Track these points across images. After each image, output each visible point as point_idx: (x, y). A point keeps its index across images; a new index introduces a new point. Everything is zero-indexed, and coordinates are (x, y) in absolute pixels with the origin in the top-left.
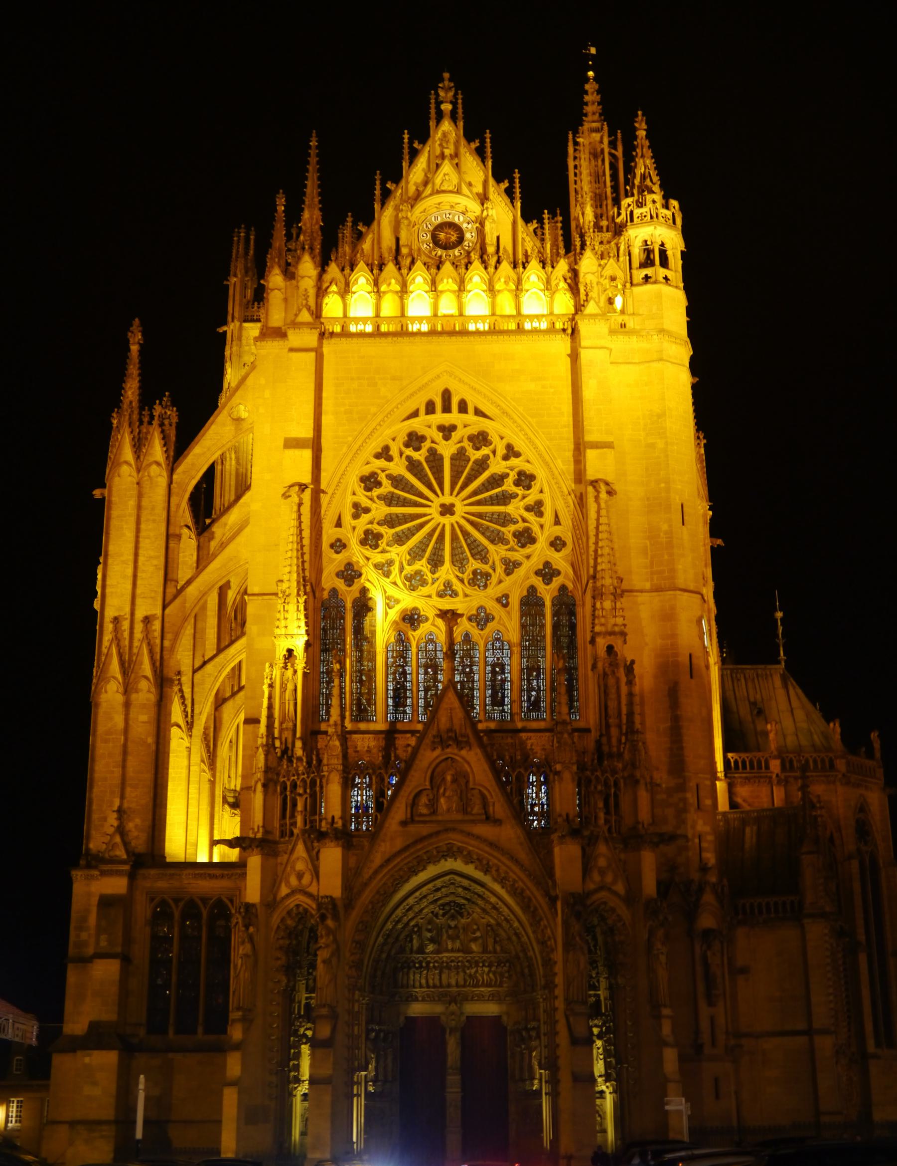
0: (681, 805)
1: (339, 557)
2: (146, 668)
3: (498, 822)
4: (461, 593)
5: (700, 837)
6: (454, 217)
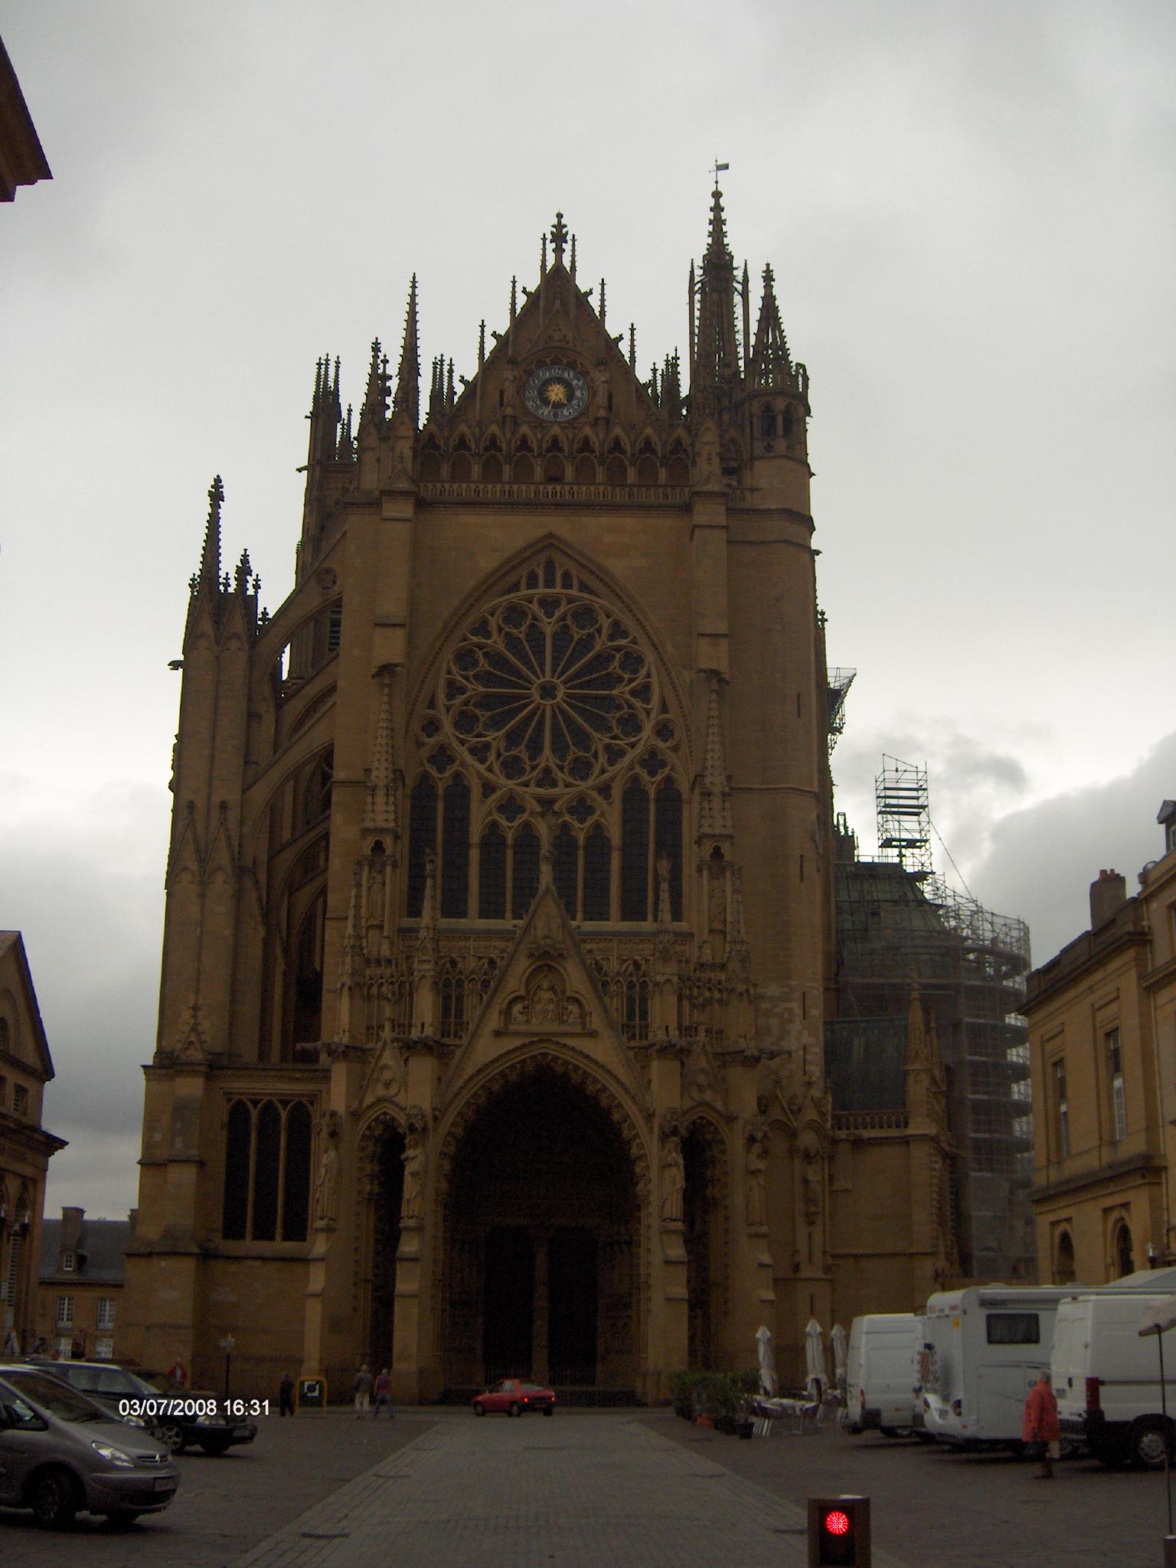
0: (786, 1015)
1: (432, 741)
3: (593, 1034)
4: (561, 784)
5: (804, 1048)
6: (563, 372)
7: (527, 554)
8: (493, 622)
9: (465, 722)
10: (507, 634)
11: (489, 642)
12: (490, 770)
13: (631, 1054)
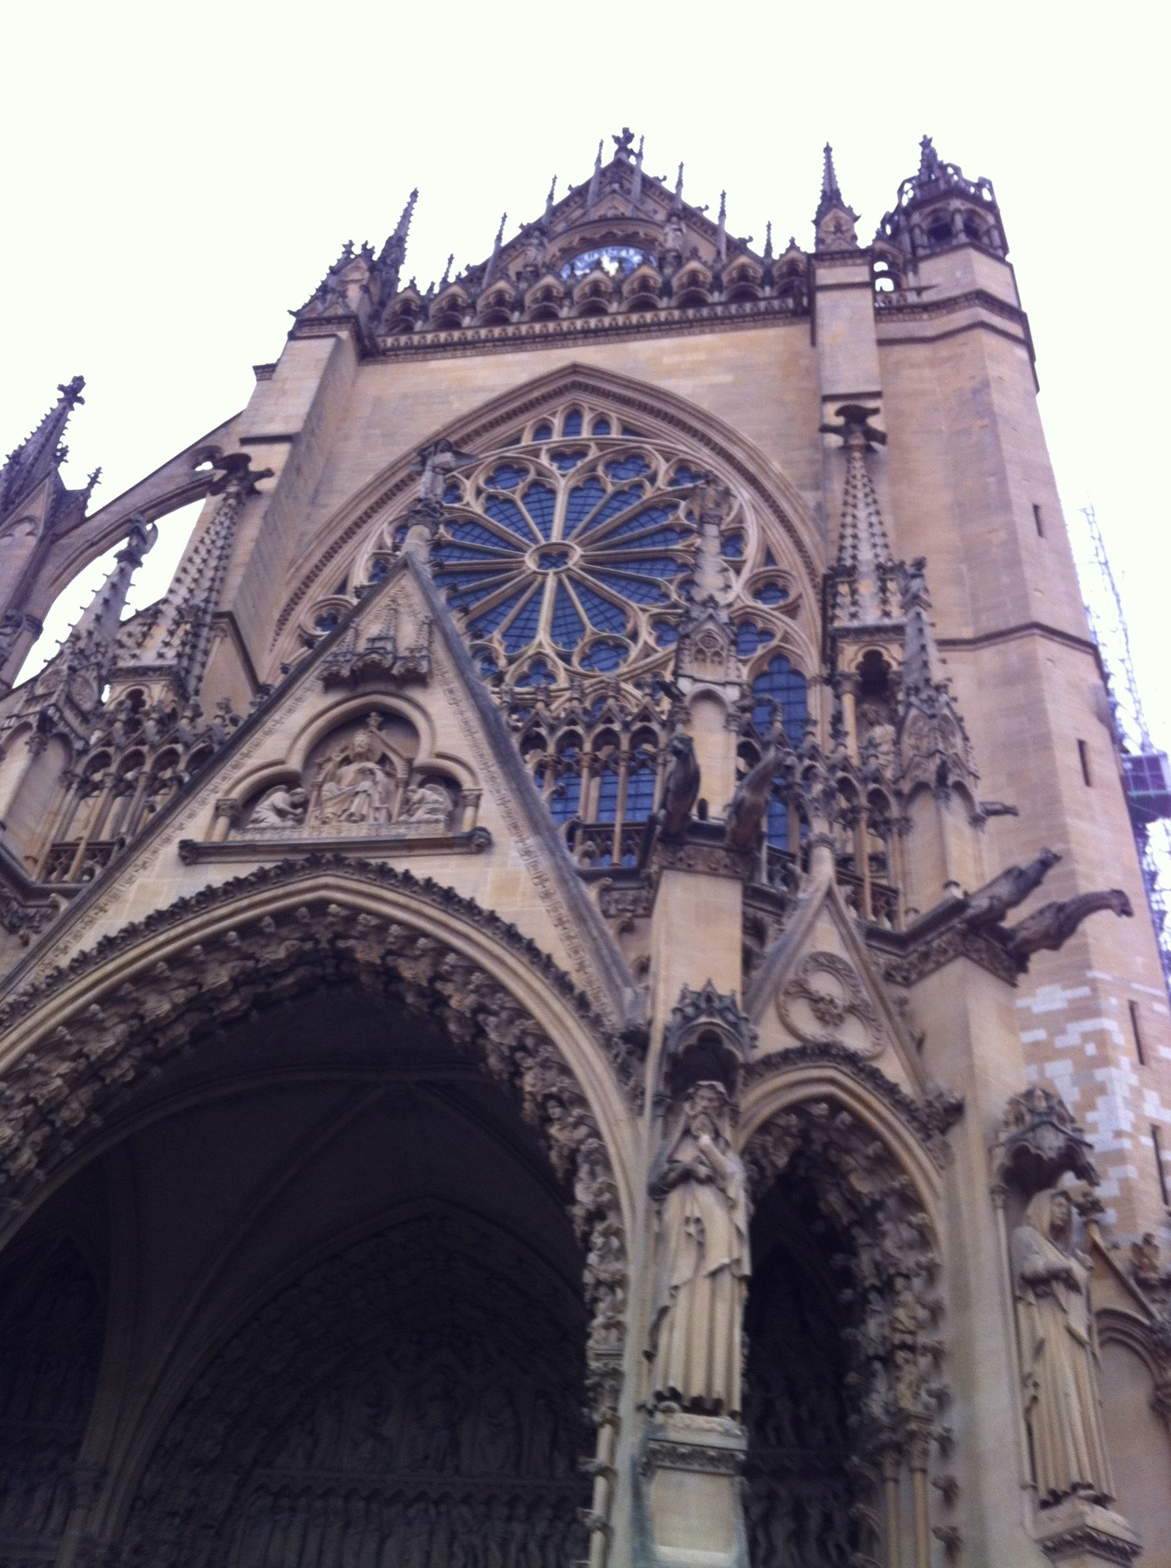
7: (536, 394)
10: (491, 498)
11: (456, 505)
13: (591, 893)
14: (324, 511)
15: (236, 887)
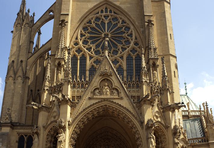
1: (77, 46)
2: (20, 73)
3: (122, 98)
8: (92, 21)
9: (85, 42)
10: (96, 23)
12: (92, 53)
13: (135, 105)
14: (73, 25)
15: (96, 103)
